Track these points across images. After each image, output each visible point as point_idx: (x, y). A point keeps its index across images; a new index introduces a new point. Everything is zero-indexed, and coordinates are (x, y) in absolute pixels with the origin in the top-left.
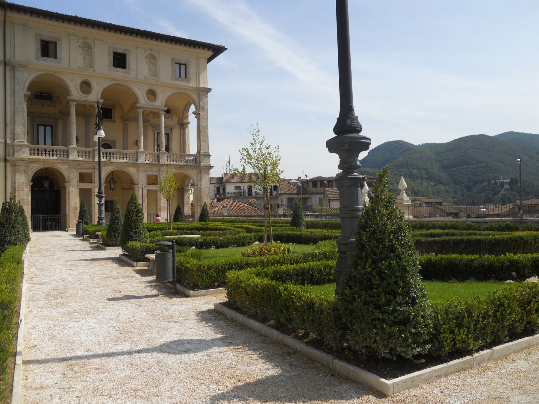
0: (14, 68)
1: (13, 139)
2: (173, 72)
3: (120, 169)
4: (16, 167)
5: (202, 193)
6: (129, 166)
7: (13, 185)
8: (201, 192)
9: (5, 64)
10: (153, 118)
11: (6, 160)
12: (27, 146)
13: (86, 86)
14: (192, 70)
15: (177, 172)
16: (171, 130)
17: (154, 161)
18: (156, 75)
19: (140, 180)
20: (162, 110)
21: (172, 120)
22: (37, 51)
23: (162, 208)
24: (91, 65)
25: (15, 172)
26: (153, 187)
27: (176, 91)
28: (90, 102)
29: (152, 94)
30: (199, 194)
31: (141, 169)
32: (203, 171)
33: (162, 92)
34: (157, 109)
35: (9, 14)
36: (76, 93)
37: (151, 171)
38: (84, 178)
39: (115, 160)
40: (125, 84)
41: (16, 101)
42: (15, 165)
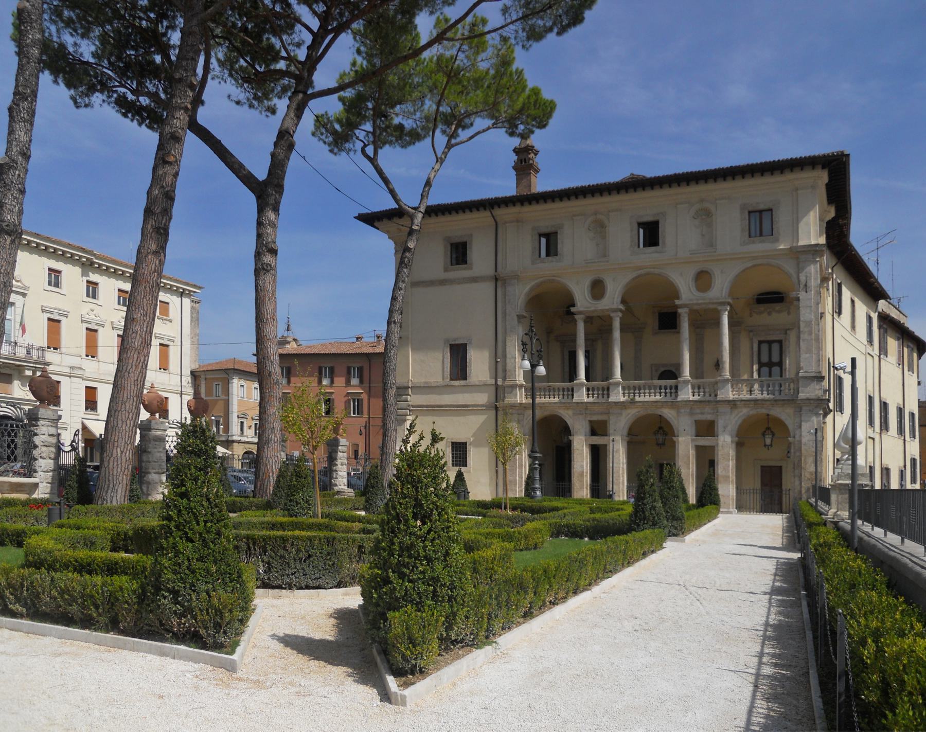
0: (504, 281)
1: (504, 379)
3: (649, 412)
5: (803, 451)
6: (662, 407)
8: (800, 450)
9: (496, 280)
10: (751, 316)
12: (521, 386)
13: (597, 288)
14: (782, 218)
15: (751, 413)
16: (786, 333)
17: (707, 395)
18: (711, 244)
20: (723, 304)
21: (789, 313)
23: (721, 479)
24: (604, 254)
26: (705, 441)
27: (750, 264)
28: (602, 310)
29: (703, 279)
30: (798, 454)
31: (682, 411)
32: (804, 408)
33: (722, 272)
34: (713, 303)
35: (498, 212)
36: (583, 302)
37: (702, 413)
38: (597, 429)
39: (642, 399)
40: (657, 271)
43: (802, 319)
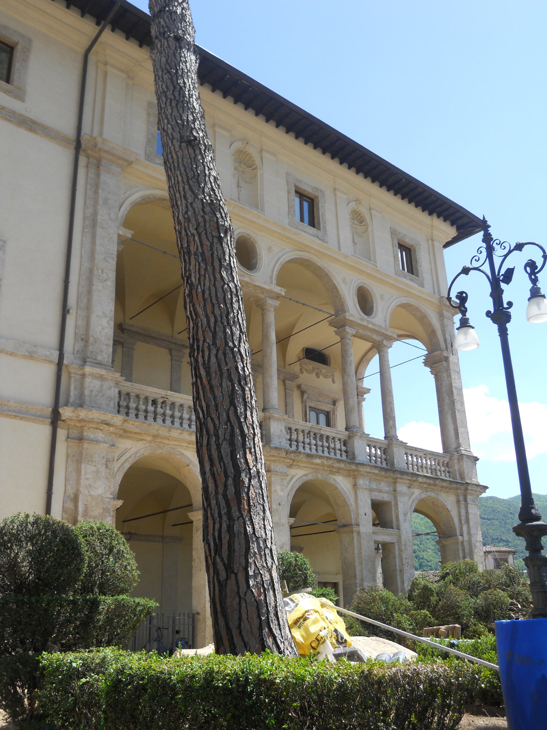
2: (395, 257)
4: (86, 445)
7: (70, 505)
9: (78, 146)
11: (55, 418)
15: (423, 496)
19: (362, 512)
22: (149, 141)
25: (79, 462)
27: (404, 300)
41: (98, 248)
42: (81, 439)
43: (454, 385)
